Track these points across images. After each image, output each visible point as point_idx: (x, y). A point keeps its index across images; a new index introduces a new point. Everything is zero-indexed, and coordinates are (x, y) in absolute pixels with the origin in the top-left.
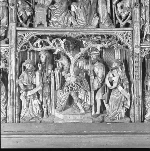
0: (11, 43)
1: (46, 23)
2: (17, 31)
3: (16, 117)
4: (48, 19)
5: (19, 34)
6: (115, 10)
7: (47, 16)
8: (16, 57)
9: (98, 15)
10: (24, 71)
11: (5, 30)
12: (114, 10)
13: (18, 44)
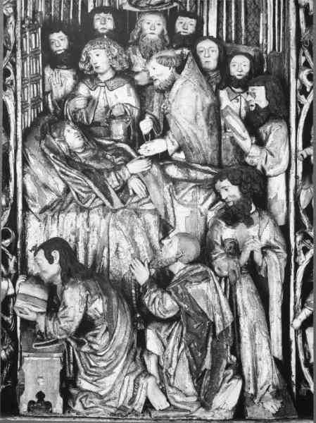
1: (60, 400)
4: (68, 385)
6: (300, 347)
7: (63, 373)
9: (239, 372)
12: (293, 347)
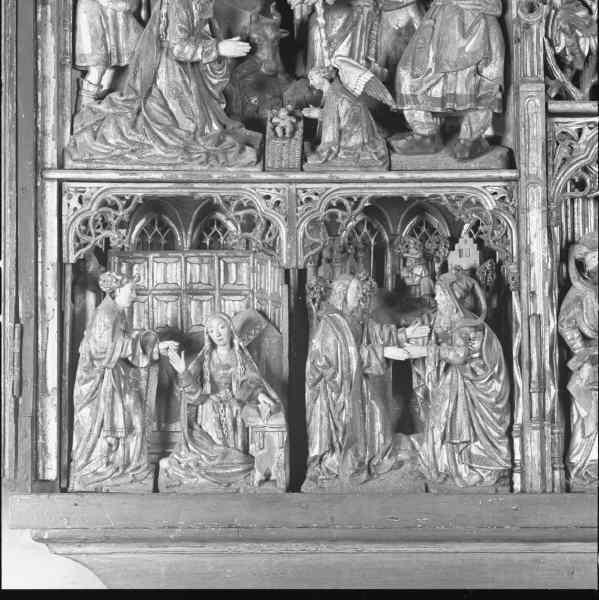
0: (526, 165)
2: (549, 114)
3: (554, 469)
5: (558, 130)
8: (548, 221)
10: (581, 279)
11: (495, 114)
13: (556, 170)
